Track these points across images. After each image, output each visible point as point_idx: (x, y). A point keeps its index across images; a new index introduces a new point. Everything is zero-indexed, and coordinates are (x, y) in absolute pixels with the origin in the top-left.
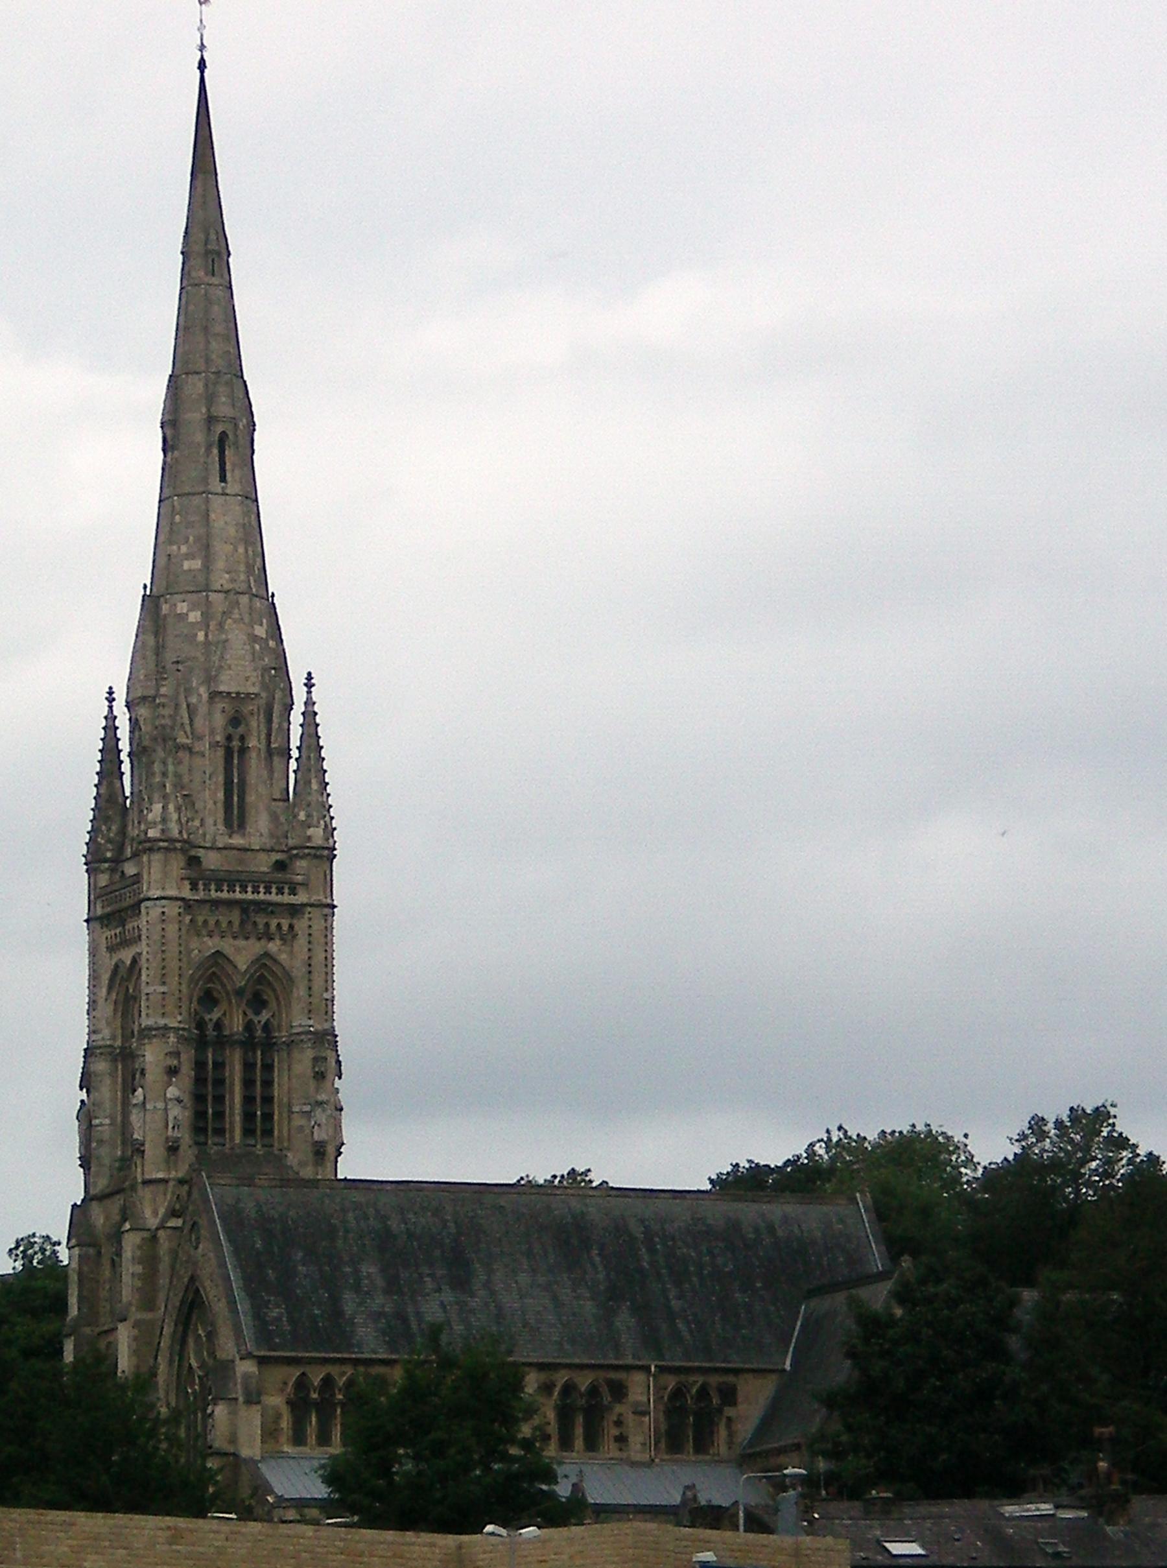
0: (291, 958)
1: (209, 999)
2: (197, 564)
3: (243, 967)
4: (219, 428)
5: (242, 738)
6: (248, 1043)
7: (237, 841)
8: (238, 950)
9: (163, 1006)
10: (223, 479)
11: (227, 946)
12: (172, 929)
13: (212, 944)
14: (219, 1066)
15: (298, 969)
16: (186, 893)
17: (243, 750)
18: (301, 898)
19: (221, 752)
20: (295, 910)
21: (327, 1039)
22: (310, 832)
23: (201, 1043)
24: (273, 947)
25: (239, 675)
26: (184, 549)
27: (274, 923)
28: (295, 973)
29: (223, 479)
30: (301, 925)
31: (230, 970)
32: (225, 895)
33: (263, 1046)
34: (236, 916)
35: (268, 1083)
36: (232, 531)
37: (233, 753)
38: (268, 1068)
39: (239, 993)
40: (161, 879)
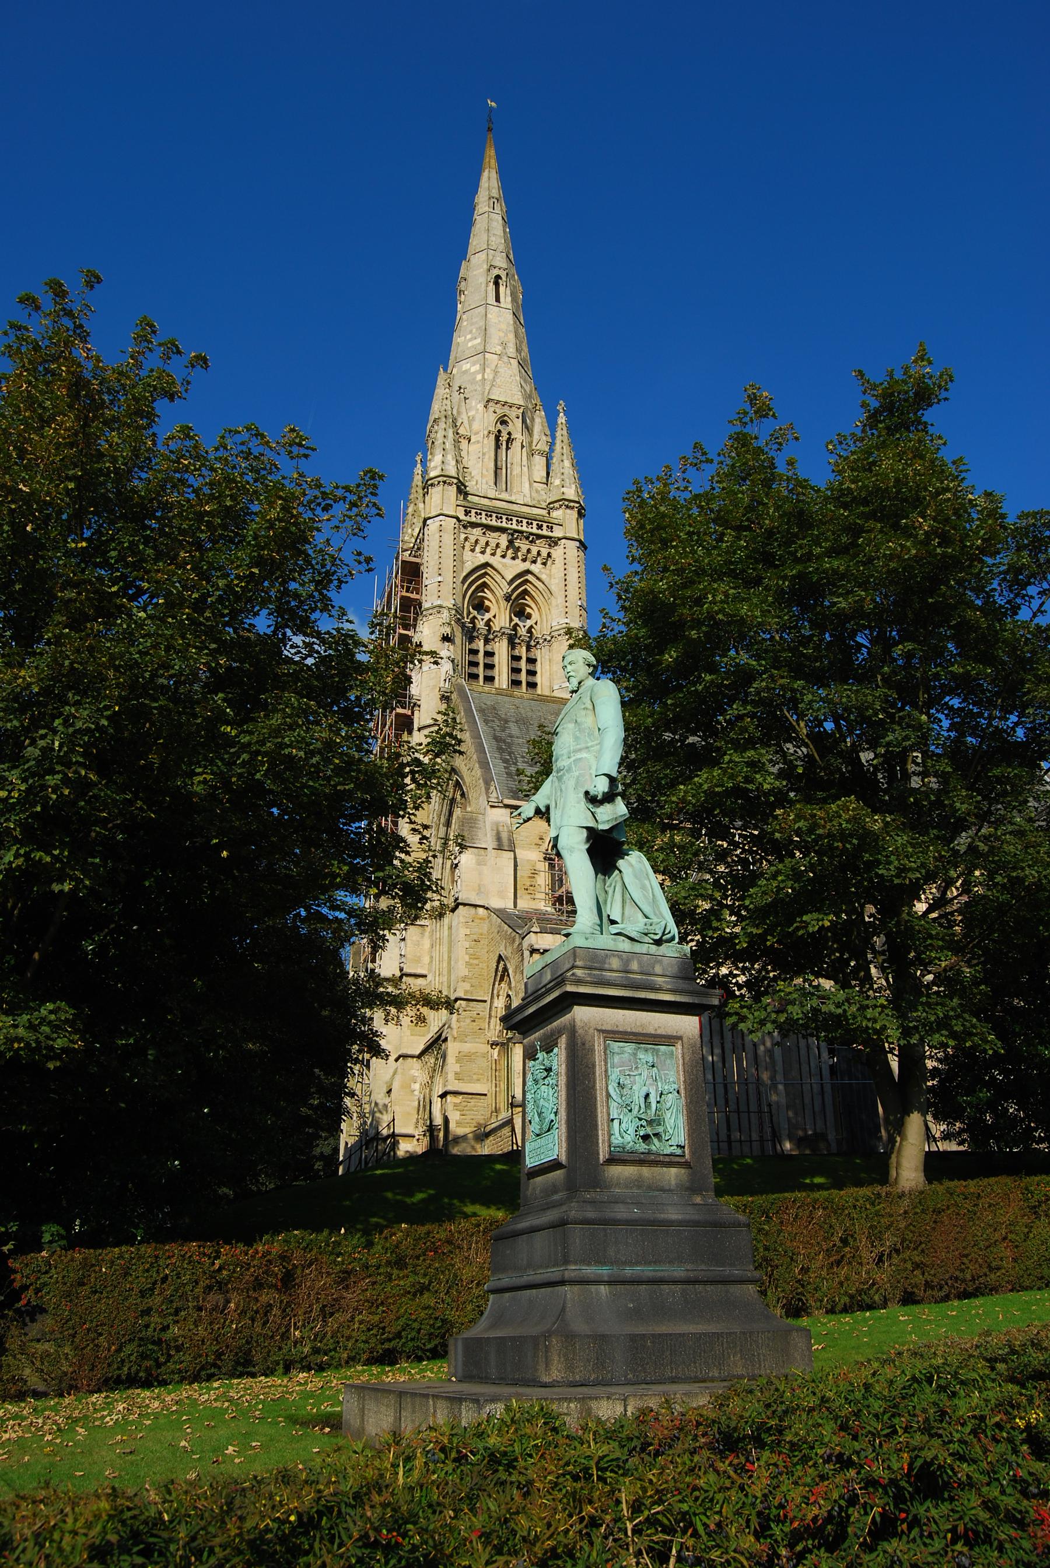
2: (479, 340)
3: (509, 577)
4: (496, 272)
5: (509, 434)
7: (504, 496)
8: (505, 565)
10: (498, 300)
11: (496, 561)
12: (448, 539)
13: (482, 559)
14: (489, 654)
16: (462, 517)
17: (510, 441)
18: (558, 533)
19: (492, 437)
20: (554, 542)
22: (564, 490)
23: (470, 634)
24: (536, 568)
26: (469, 337)
27: (534, 550)
28: (553, 588)
29: (498, 300)
30: (557, 553)
31: (498, 578)
32: (494, 523)
34: (504, 540)
35: (532, 673)
36: (504, 326)
38: (532, 661)
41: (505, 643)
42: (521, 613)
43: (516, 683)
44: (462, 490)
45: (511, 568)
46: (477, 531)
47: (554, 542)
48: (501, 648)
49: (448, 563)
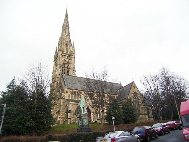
0: (71, 61)
1: (64, 64)
6: (67, 68)
9: (60, 62)
11: (66, 59)
12: (61, 57)
13: (64, 59)
15: (72, 62)
17: (68, 46)
20: (72, 57)
21: (74, 68)
23: (63, 67)
25: (67, 40)
33: (68, 69)
37: (67, 45)
39: (67, 63)
40: (60, 52)
41: (66, 68)
42: (68, 65)
43: (67, 74)
44: (62, 51)
45: (67, 60)
46: (64, 56)
47: (72, 57)
48: (66, 69)
49: (60, 60)
